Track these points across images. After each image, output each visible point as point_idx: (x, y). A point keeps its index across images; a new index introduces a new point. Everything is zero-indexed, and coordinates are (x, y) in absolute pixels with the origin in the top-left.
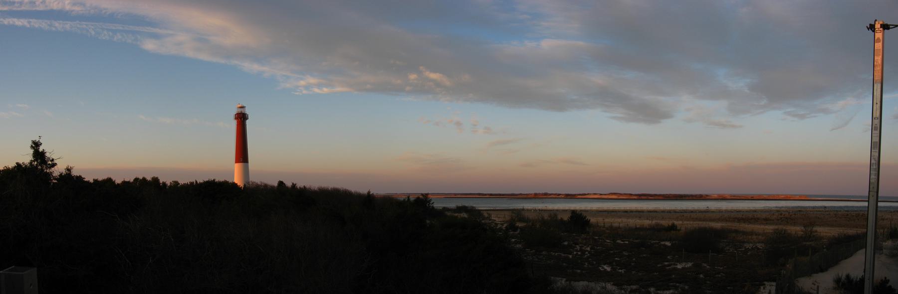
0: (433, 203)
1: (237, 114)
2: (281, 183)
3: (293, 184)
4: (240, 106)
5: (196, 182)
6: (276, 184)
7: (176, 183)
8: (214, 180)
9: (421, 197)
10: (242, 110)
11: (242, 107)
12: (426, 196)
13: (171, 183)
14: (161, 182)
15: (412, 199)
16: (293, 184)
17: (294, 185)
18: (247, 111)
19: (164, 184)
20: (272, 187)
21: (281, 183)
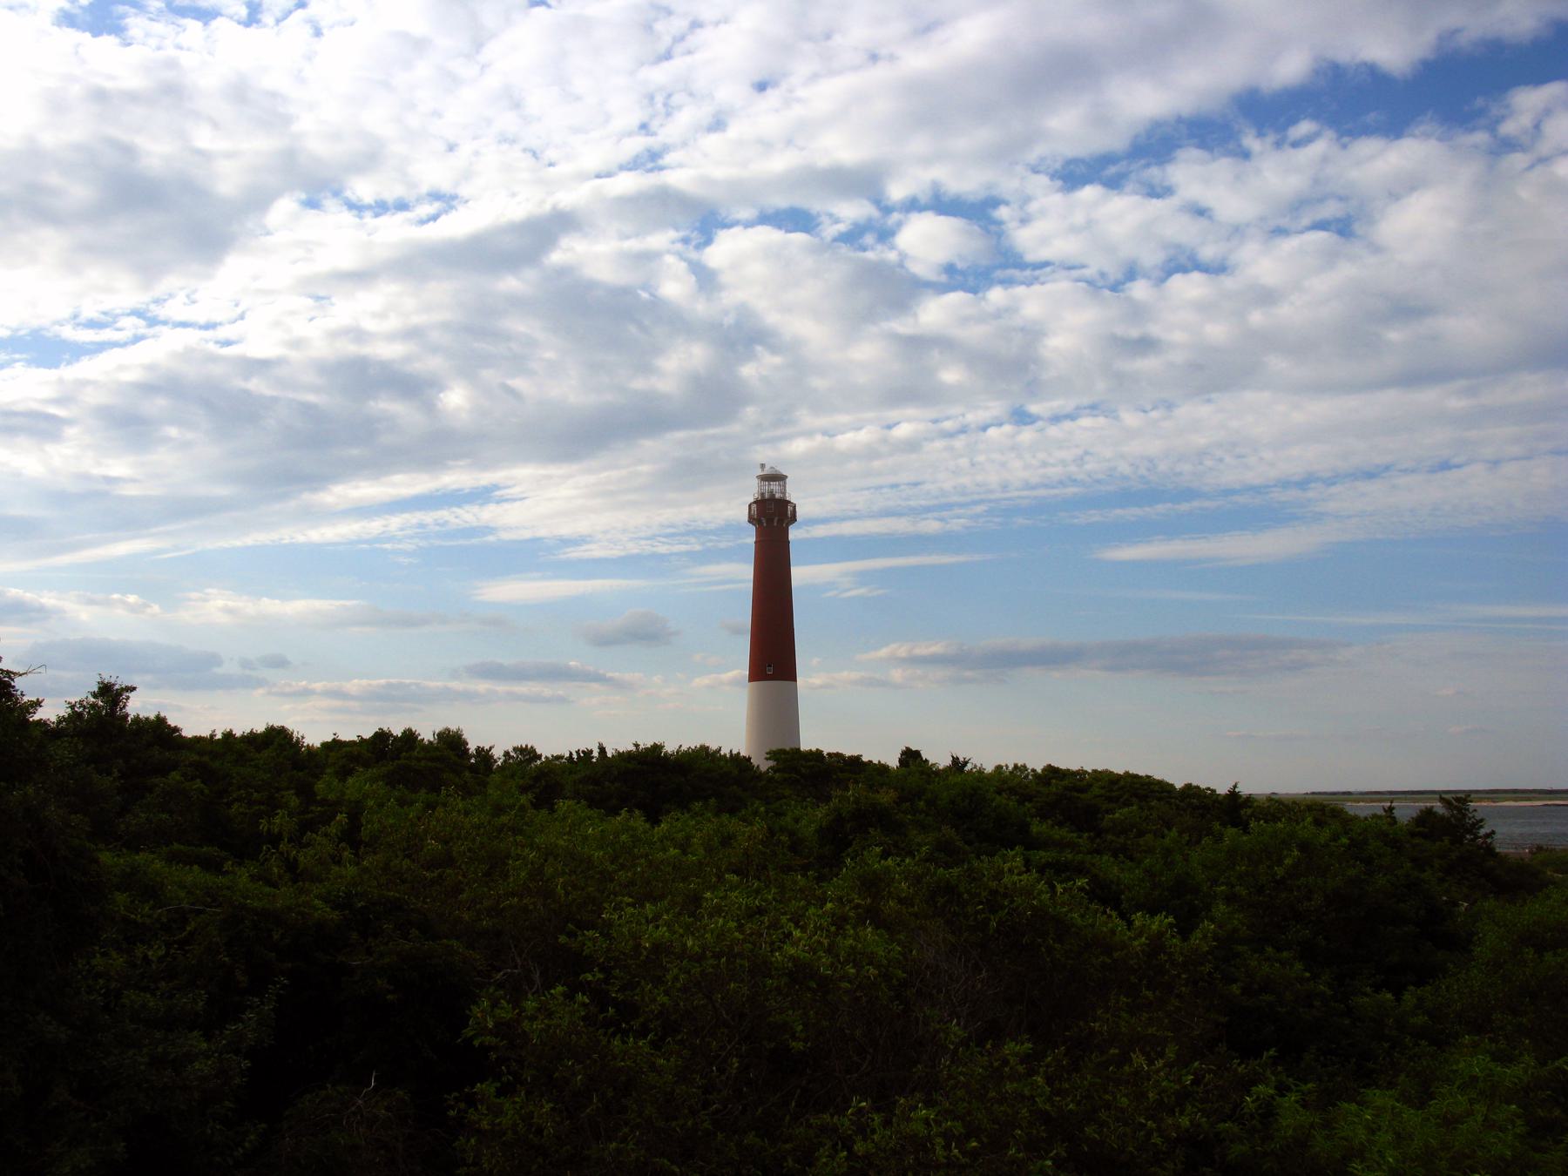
0: (1488, 835)
1: (755, 502)
2: (910, 757)
3: (955, 760)
4: (767, 471)
5: (602, 750)
6: (893, 762)
7: (528, 754)
8: (657, 748)
9: (1438, 807)
10: (775, 486)
11: (779, 478)
12: (1458, 802)
13: (507, 754)
14: (472, 747)
15: (1406, 813)
16: (955, 760)
17: (958, 765)
18: (793, 495)
19: (484, 755)
20: (882, 769)
21: (910, 757)
